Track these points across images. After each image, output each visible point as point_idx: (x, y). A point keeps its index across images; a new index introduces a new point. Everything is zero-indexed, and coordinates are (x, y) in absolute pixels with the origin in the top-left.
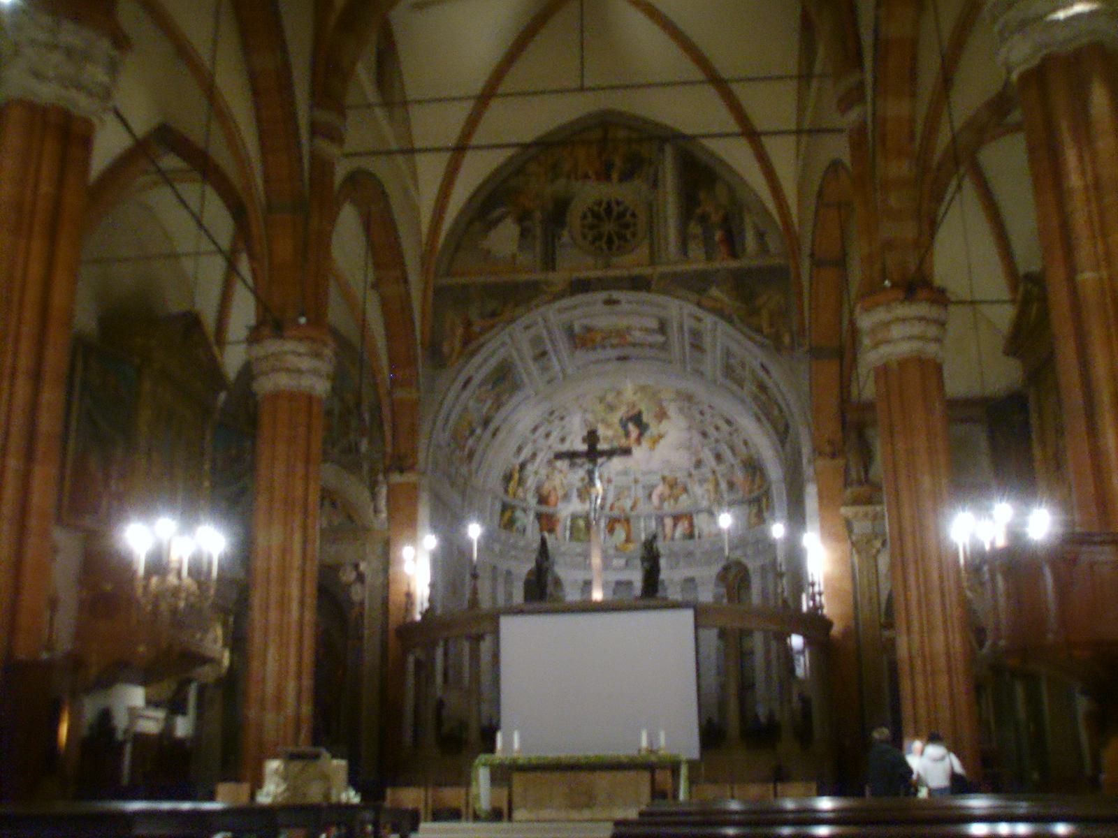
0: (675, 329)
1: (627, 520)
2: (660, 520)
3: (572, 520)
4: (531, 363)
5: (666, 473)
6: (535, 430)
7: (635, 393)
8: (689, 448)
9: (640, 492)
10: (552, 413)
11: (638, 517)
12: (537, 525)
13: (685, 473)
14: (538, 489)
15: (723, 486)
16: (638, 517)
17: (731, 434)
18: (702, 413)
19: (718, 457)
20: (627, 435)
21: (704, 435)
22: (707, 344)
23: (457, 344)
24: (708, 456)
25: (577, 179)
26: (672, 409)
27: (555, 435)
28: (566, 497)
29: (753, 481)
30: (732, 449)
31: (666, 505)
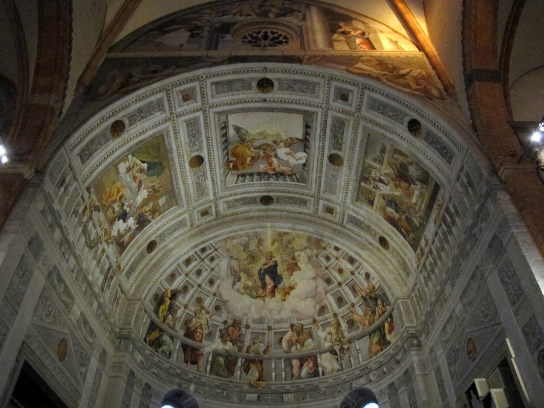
0: (318, 131)
1: (261, 362)
2: (288, 361)
3: (213, 357)
4: (187, 166)
5: (295, 322)
6: (188, 262)
7: (273, 244)
8: (314, 298)
9: (272, 338)
10: (203, 250)
11: (269, 359)
12: (182, 355)
13: (311, 320)
14: (187, 323)
15: (344, 326)
16: (269, 359)
17: (352, 273)
18: (328, 258)
19: (340, 301)
20: (264, 286)
21: (328, 281)
22: (345, 154)
23: (115, 87)
24: (331, 301)
25: (241, 15)
26: (302, 258)
27: (205, 274)
28: (210, 335)
29: (374, 312)
30: (354, 291)
31: (293, 349)
